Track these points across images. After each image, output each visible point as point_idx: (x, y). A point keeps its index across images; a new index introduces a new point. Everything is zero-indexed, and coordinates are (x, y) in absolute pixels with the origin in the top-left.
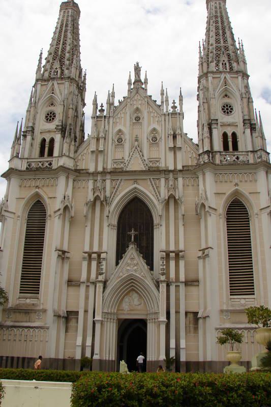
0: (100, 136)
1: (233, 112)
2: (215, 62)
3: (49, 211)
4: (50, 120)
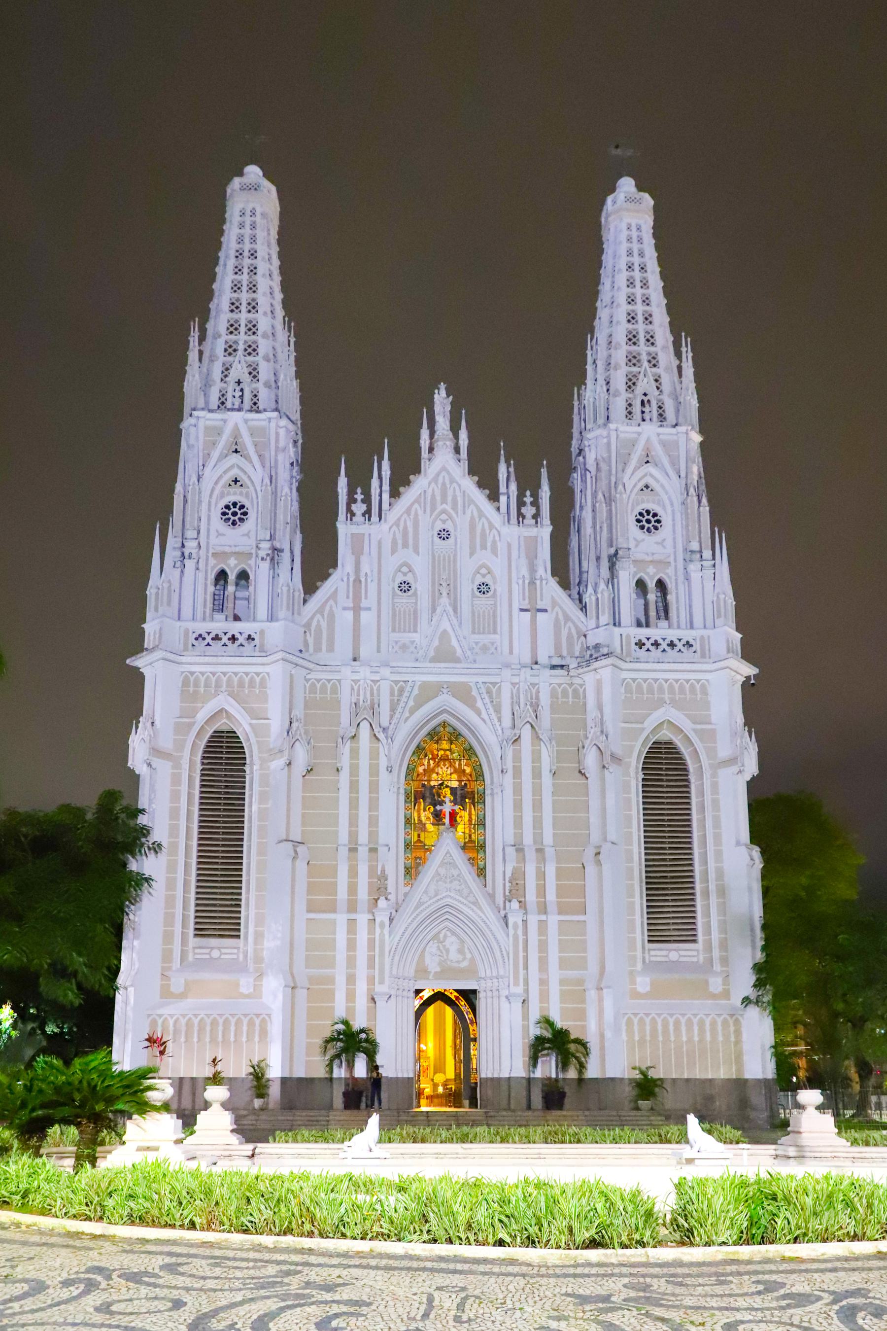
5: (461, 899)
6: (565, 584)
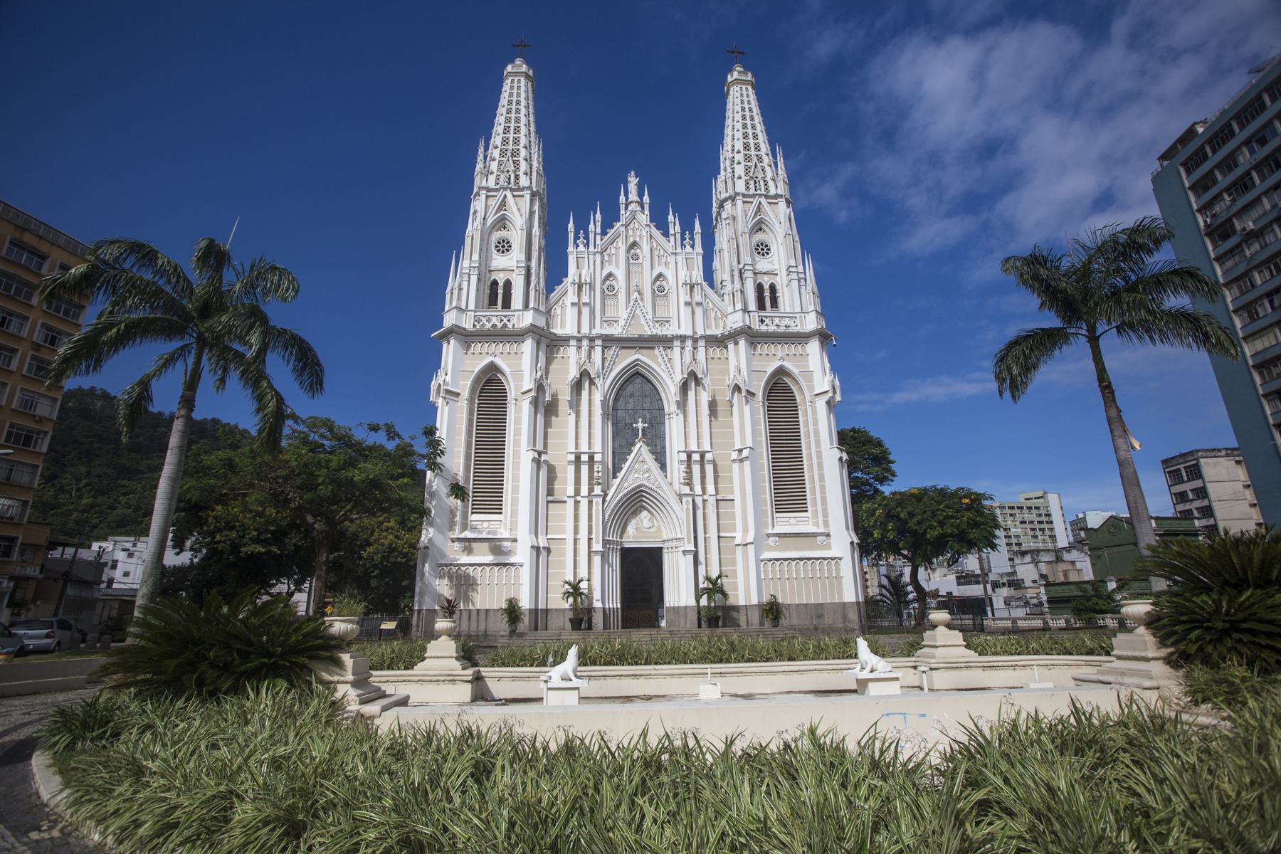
0: (583, 281)
1: (770, 255)
2: (744, 178)
3: (512, 394)
4: (503, 252)
5: (650, 485)
6: (712, 285)
